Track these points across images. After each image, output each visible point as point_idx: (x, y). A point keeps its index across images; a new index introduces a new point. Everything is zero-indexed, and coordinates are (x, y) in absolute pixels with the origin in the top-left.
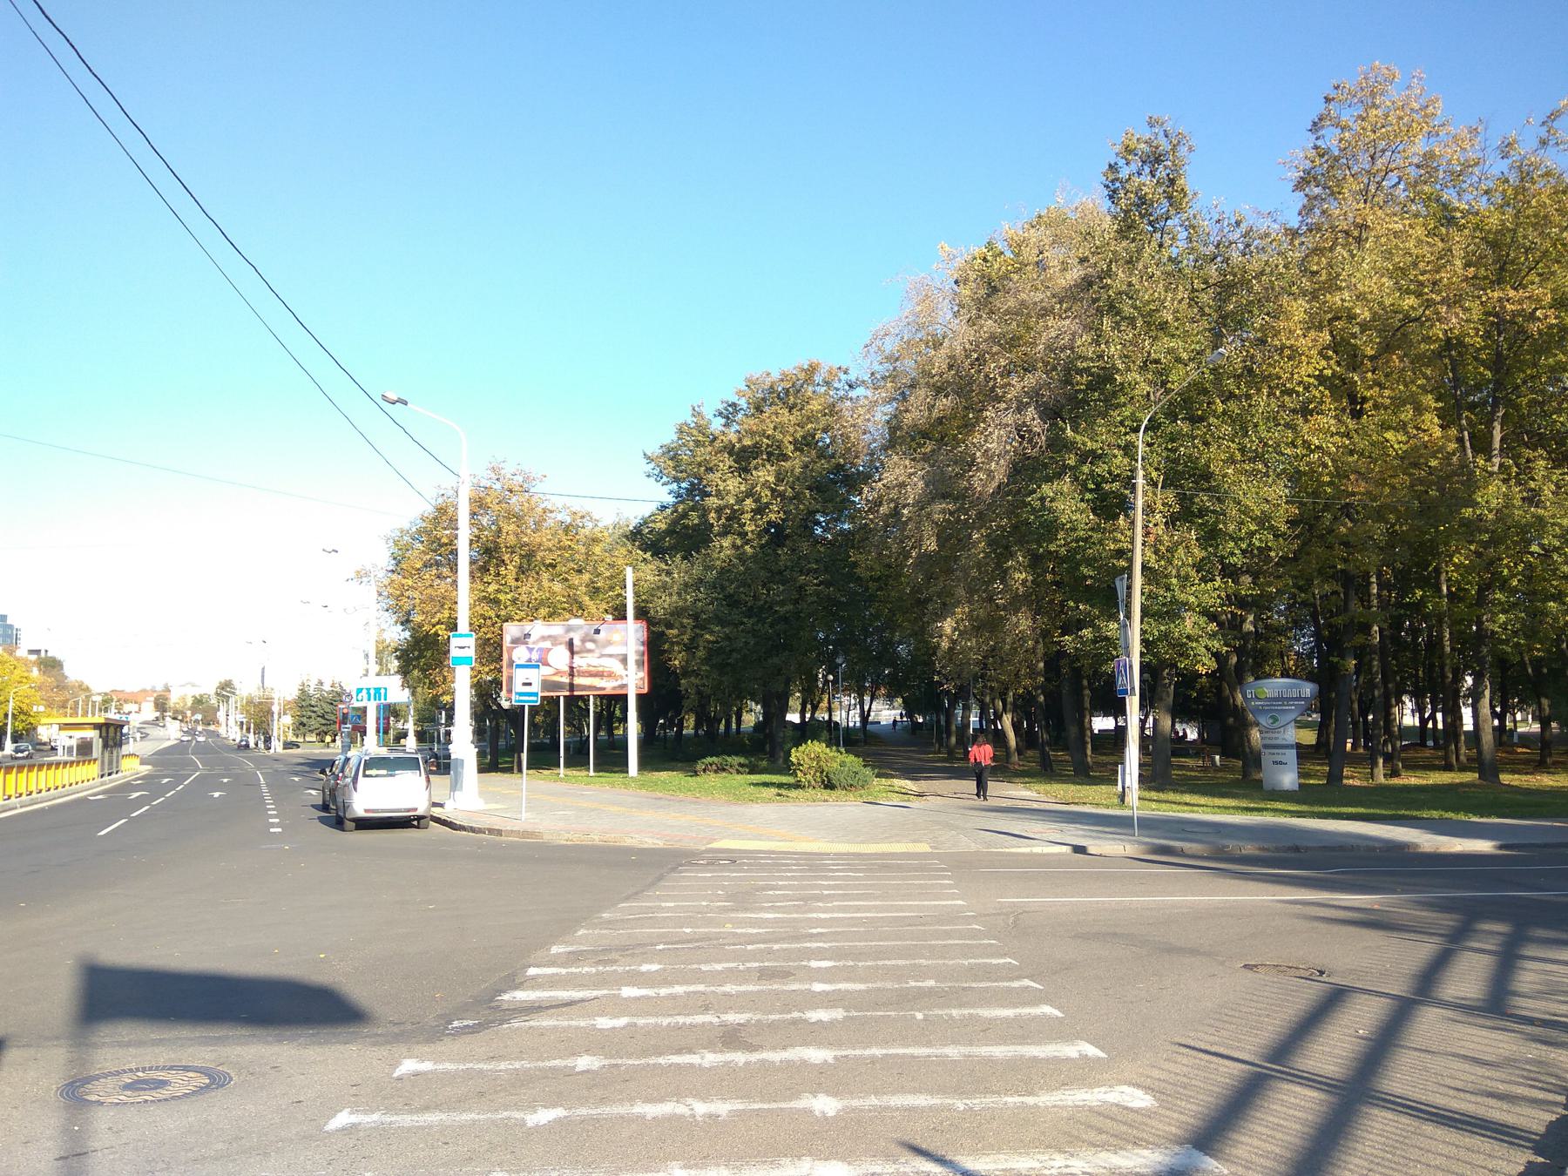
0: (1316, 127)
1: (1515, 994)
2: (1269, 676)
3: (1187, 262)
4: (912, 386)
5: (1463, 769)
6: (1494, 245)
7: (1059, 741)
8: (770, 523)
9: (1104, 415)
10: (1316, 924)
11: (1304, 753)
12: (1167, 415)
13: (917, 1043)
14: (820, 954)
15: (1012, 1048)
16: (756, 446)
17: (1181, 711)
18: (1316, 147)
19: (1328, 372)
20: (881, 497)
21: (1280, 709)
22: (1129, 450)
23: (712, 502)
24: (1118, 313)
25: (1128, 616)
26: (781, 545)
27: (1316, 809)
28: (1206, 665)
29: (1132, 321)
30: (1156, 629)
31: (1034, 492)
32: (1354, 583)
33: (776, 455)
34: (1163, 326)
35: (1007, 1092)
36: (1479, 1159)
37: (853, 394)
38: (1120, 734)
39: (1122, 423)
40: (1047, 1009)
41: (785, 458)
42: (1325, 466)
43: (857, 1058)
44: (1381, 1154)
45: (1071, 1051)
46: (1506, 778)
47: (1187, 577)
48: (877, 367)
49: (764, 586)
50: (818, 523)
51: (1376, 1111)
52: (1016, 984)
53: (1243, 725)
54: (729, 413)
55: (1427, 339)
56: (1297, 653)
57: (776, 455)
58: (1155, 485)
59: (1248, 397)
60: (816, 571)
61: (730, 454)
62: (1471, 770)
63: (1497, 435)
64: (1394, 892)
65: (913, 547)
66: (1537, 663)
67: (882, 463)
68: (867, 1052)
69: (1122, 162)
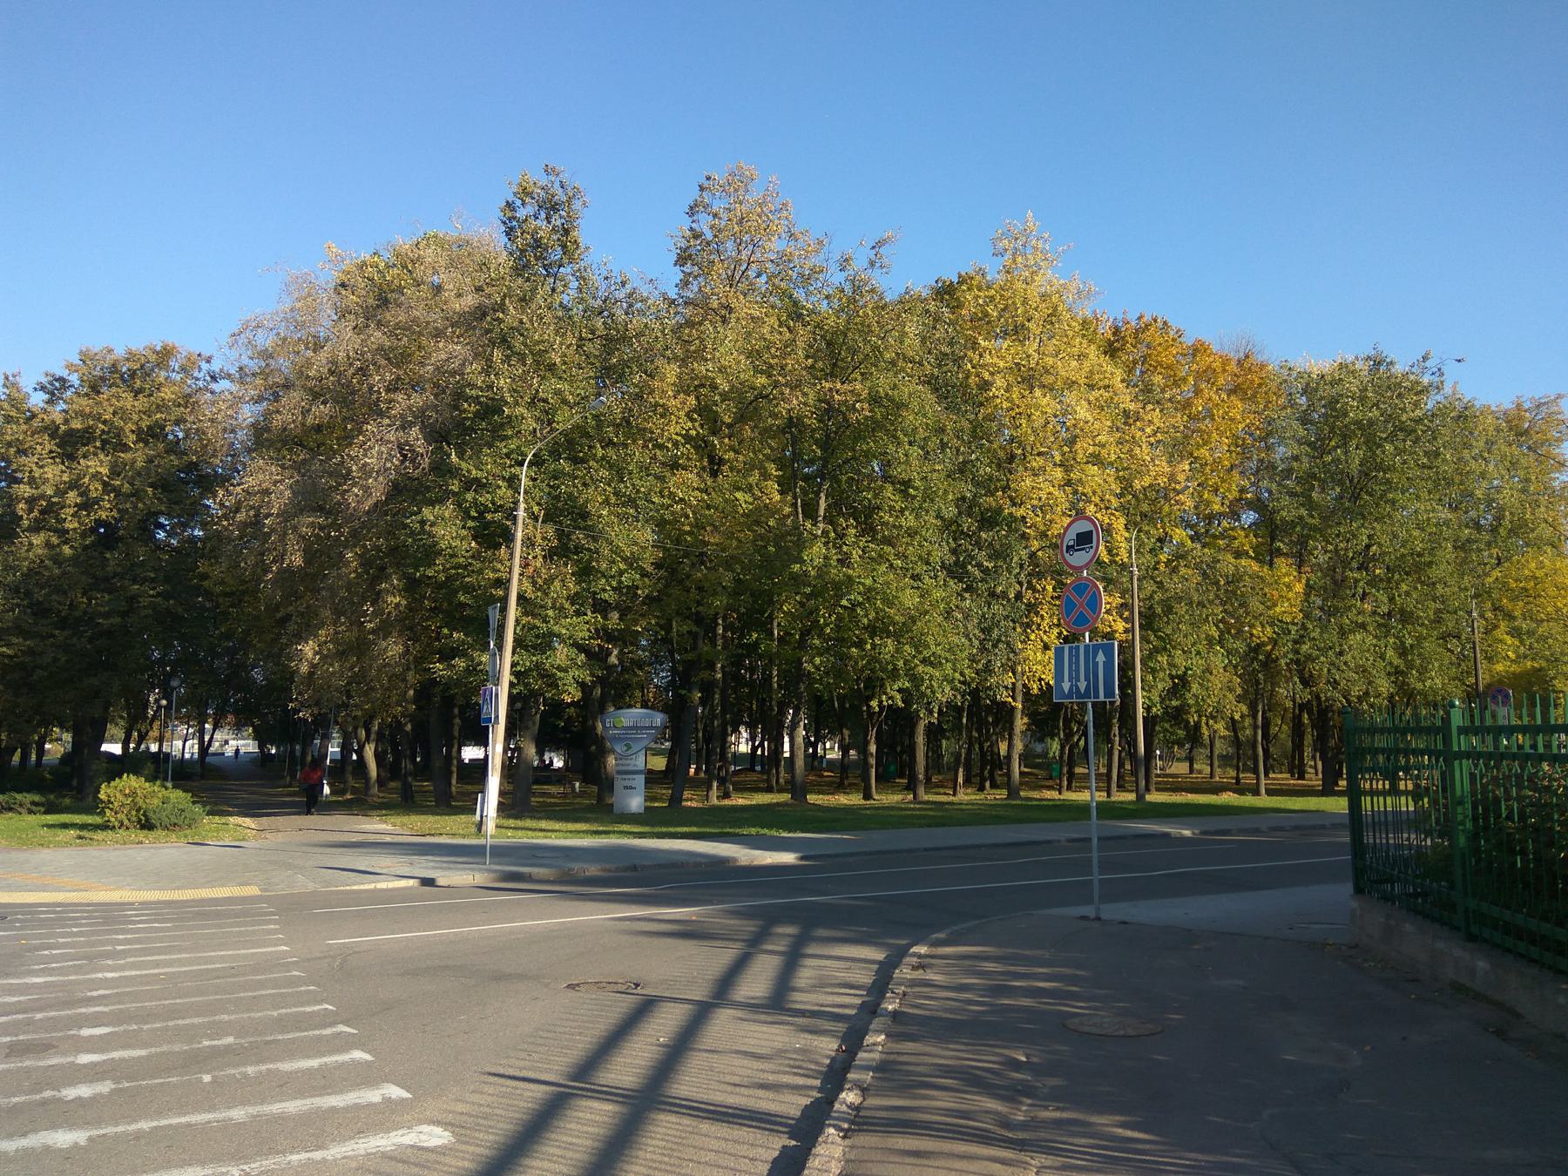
0: (692, 211)
1: (794, 989)
2: (630, 706)
3: (577, 311)
4: (287, 386)
5: (780, 791)
6: (829, 344)
7: (423, 771)
8: (99, 523)
9: (490, 446)
10: (640, 939)
11: (652, 778)
12: (551, 453)
13: (198, 1108)
14: (95, 1020)
15: (308, 1101)
16: (87, 430)
17: (545, 742)
18: (691, 229)
19: (693, 433)
20: (239, 503)
21: (635, 738)
22: (513, 481)
23: (25, 490)
24: (509, 348)
25: (500, 646)
26: (110, 548)
27: (657, 829)
28: (571, 694)
29: (522, 359)
30: (528, 661)
31: (416, 514)
32: (706, 624)
33: (113, 443)
34: (552, 367)
35: (293, 1150)
36: (743, 1150)
37: (214, 386)
38: (481, 767)
39: (507, 456)
40: (358, 1055)
41: (125, 448)
42: (687, 517)
43: (117, 1136)
44: (659, 1158)
45: (373, 1096)
46: (812, 798)
47: (562, 608)
48: (245, 361)
49: (84, 594)
50: (162, 526)
51: (662, 1116)
52: (328, 1031)
53: (603, 752)
54: (55, 388)
55: (775, 416)
56: (656, 686)
57: (113, 443)
58: (536, 519)
59: (626, 446)
60: (153, 580)
61: (52, 437)
62: (786, 791)
63: (823, 505)
64: (710, 903)
65: (275, 561)
66: (842, 699)
67: (244, 465)
68: (134, 1127)
69: (518, 203)
